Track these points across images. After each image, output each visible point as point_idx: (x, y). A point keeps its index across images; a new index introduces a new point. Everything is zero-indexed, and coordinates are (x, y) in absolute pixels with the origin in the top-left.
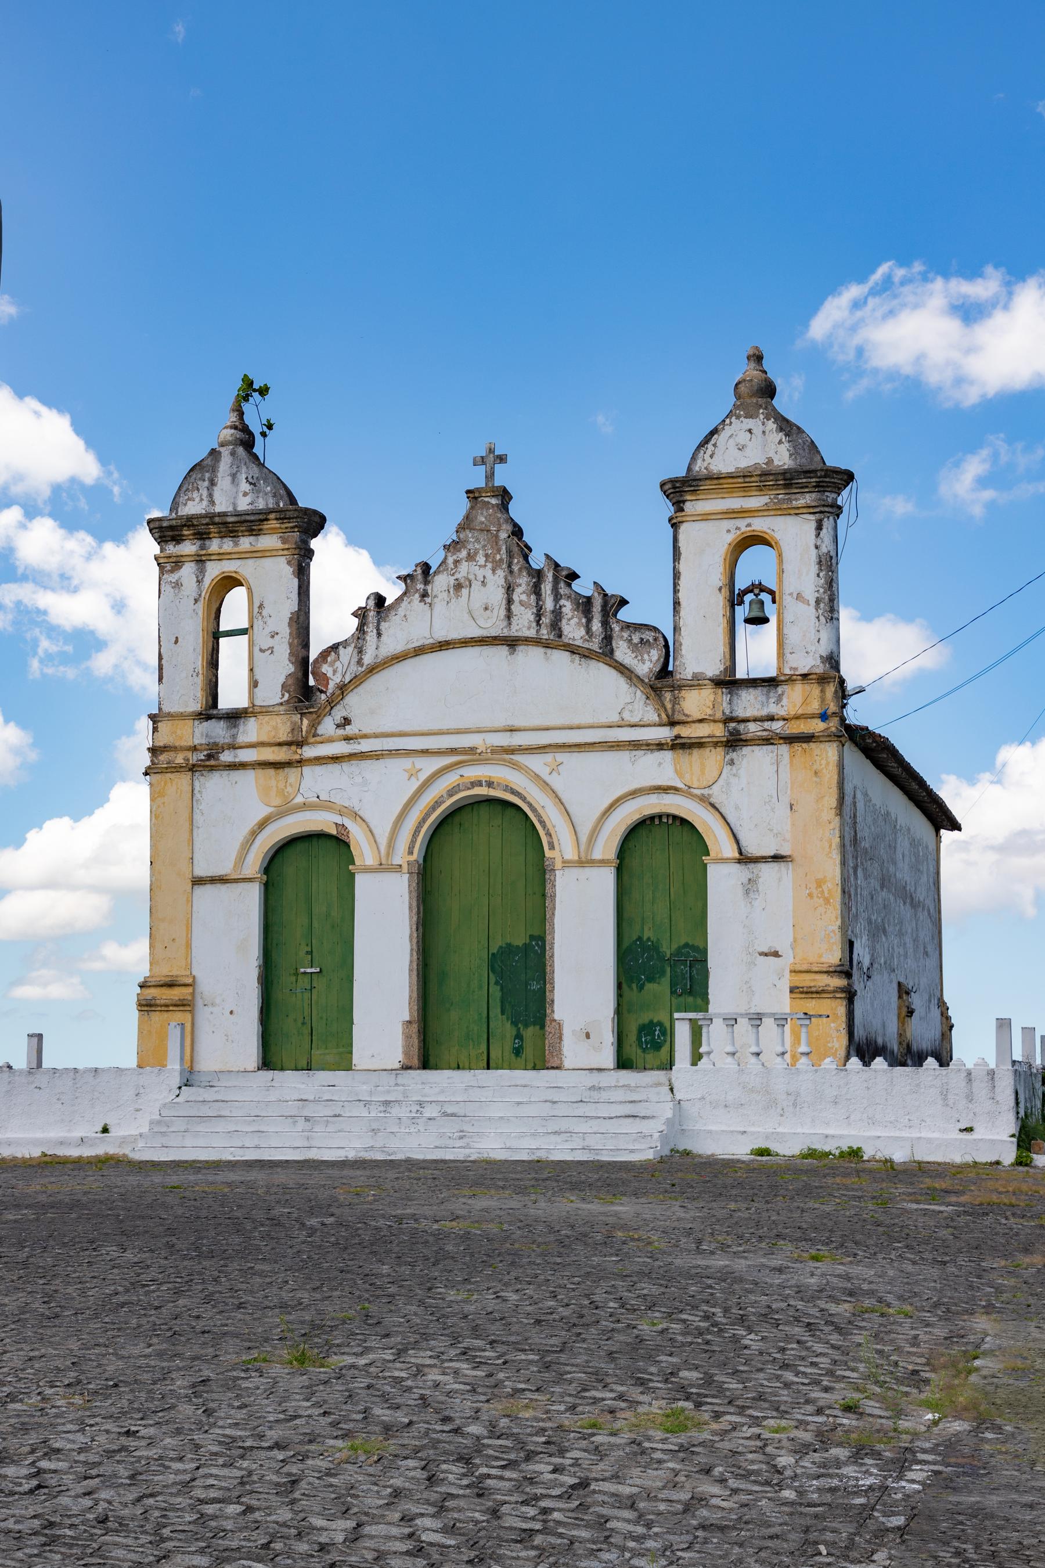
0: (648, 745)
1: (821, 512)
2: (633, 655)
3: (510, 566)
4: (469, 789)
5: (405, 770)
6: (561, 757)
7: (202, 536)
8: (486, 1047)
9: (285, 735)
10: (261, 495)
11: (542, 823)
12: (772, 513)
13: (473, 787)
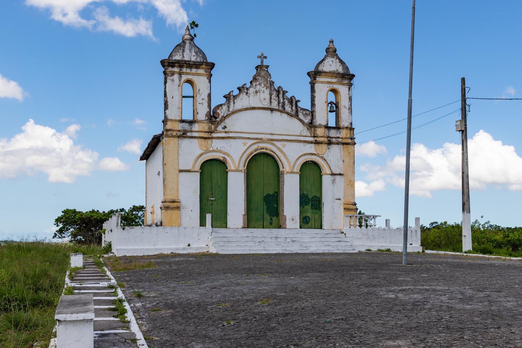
0: (308, 142)
1: (350, 85)
2: (304, 117)
3: (271, 88)
4: (260, 150)
5: (243, 143)
6: (285, 143)
7: (181, 67)
8: (263, 222)
9: (207, 129)
10: (199, 57)
11: (281, 161)
12: (338, 84)
13: (262, 149)
